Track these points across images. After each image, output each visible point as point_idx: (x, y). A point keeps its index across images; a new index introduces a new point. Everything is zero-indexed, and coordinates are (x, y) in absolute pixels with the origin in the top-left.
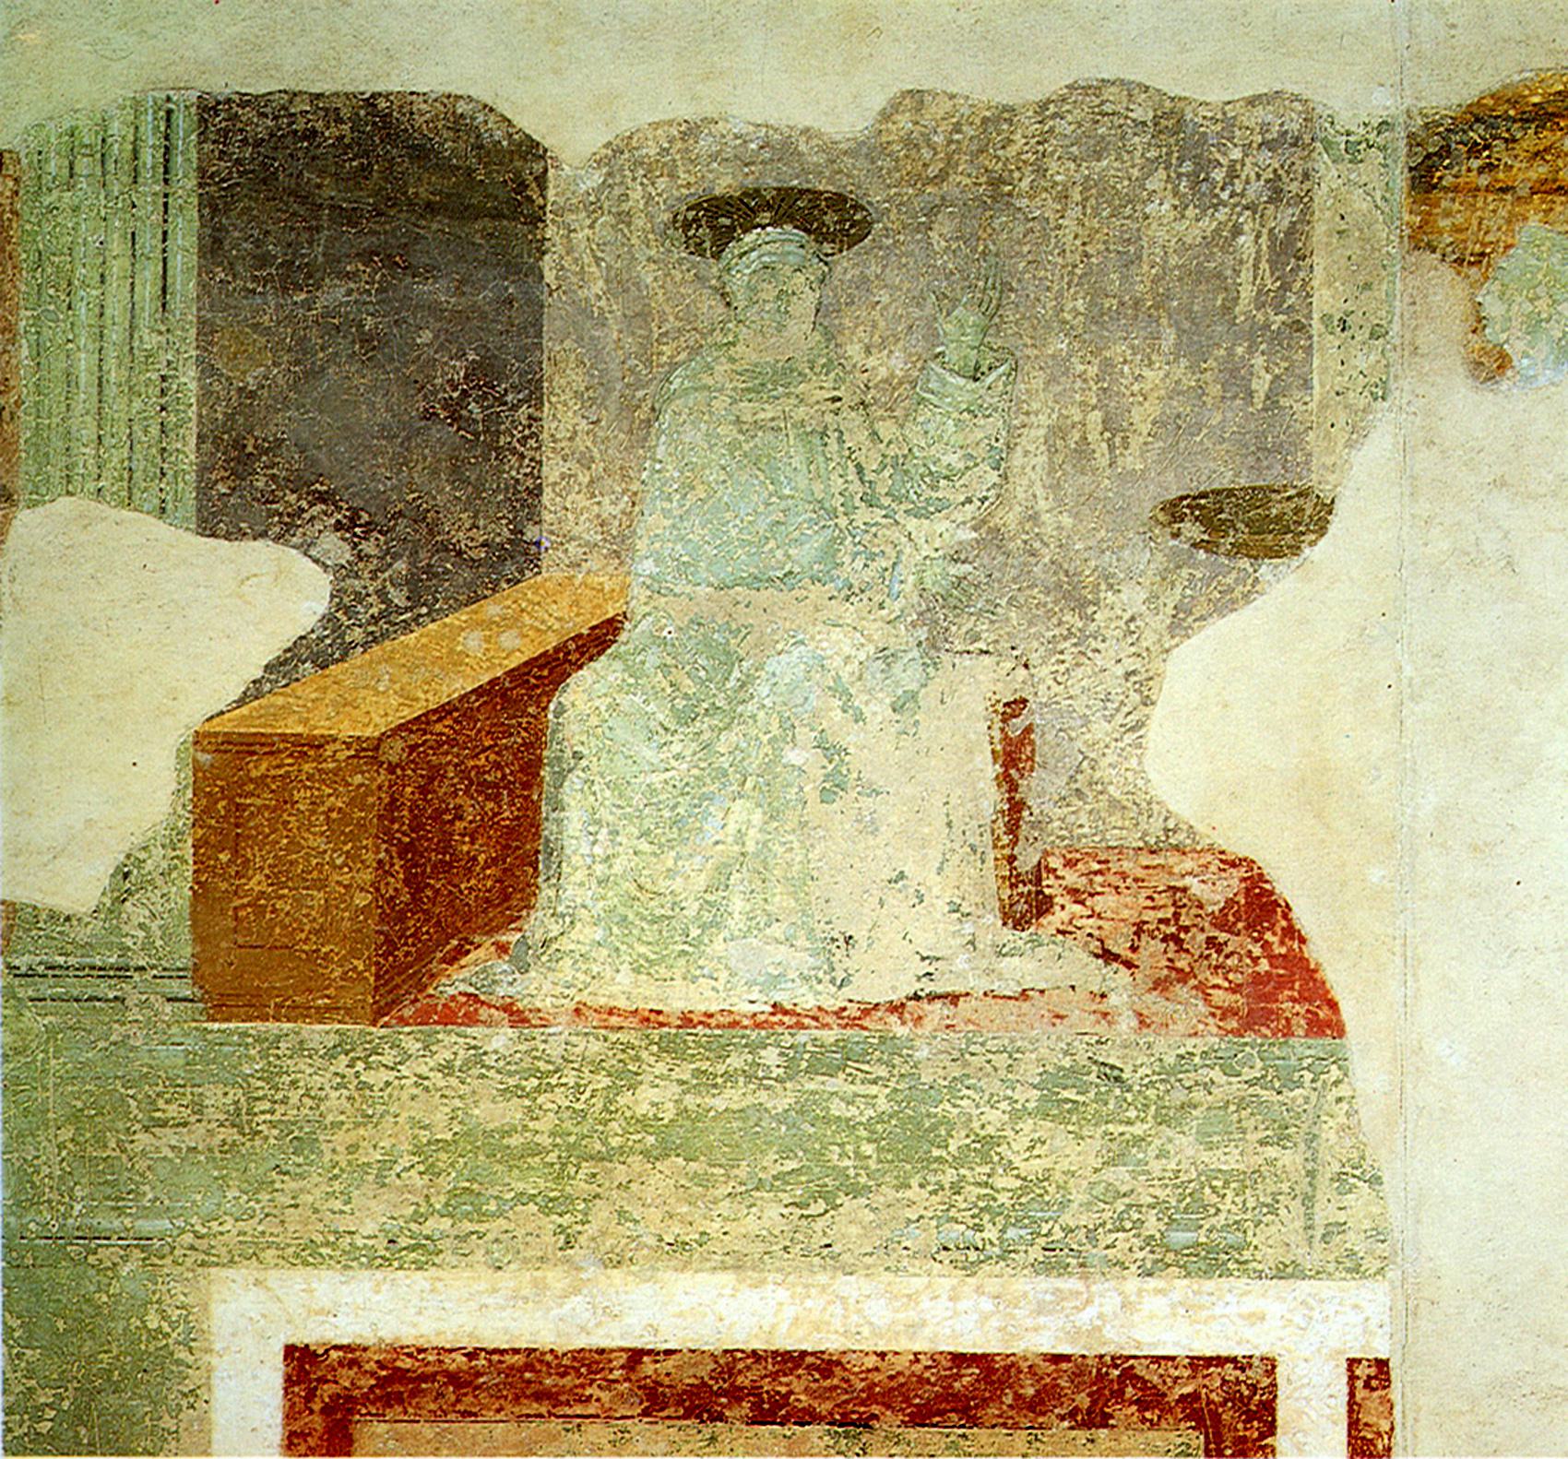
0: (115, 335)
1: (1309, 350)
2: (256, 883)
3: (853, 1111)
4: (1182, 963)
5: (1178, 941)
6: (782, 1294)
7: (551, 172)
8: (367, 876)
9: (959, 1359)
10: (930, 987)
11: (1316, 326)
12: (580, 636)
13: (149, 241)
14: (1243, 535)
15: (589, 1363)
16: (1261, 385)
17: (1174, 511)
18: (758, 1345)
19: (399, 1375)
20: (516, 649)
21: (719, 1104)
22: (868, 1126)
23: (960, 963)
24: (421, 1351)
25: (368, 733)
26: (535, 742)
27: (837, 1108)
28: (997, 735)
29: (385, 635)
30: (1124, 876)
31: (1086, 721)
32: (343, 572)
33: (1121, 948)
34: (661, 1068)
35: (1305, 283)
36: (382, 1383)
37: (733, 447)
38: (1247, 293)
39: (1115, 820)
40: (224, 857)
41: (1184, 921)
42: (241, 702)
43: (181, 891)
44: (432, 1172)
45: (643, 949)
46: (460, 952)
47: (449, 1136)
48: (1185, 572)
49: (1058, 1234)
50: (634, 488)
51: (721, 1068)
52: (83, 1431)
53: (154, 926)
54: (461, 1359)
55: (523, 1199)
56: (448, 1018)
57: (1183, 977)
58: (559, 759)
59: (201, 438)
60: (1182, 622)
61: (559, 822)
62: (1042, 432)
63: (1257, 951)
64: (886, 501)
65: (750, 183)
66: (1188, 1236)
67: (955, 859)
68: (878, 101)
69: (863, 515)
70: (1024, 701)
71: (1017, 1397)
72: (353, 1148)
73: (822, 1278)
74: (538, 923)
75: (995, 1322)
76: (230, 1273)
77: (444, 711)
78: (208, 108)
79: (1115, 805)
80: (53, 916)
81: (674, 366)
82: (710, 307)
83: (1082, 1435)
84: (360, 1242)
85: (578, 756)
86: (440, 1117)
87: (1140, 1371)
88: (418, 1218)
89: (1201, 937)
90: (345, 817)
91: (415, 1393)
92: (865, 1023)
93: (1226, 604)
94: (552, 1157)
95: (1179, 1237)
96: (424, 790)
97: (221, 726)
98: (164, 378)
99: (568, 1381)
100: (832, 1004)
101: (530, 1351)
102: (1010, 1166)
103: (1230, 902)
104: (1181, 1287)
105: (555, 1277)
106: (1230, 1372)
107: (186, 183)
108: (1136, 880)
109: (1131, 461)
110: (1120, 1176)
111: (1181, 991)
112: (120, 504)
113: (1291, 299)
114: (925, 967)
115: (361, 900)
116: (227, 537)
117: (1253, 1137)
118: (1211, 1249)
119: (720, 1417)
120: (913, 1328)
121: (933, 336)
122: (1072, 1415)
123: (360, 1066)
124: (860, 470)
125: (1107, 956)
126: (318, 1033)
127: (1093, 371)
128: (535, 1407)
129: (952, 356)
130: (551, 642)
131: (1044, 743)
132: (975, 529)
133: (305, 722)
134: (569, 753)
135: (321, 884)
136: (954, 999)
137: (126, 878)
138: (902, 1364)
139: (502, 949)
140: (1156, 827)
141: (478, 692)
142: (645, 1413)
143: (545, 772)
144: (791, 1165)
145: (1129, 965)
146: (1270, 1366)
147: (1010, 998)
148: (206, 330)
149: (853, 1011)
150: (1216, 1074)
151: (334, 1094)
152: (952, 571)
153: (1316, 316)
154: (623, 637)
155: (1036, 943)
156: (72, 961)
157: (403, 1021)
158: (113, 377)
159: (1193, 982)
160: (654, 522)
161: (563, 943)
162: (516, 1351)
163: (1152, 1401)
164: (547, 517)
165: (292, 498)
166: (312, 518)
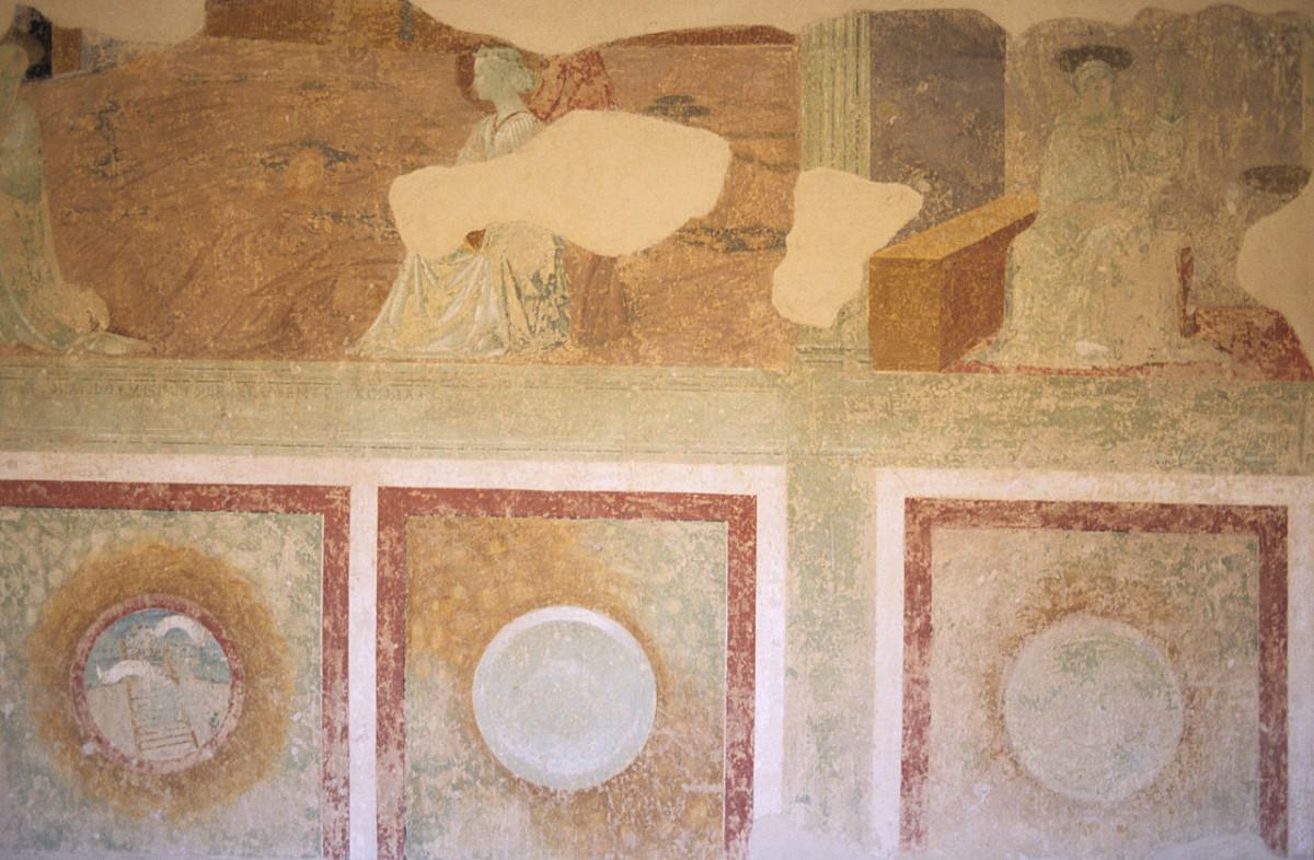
0: (838, 105)
1: (1301, 113)
2: (893, 317)
3: (1122, 409)
4: (1251, 351)
5: (1249, 343)
6: (1095, 481)
7: (1007, 40)
8: (937, 314)
9: (1163, 506)
10: (1152, 360)
11: (1304, 103)
12: (1019, 221)
13: (851, 69)
14: (1275, 184)
15: (1021, 506)
16: (1282, 125)
17: (1247, 175)
18: (1086, 499)
19: (949, 510)
20: (996, 225)
21: (1072, 405)
22: (1129, 414)
23: (1165, 351)
24: (957, 500)
25: (937, 258)
26: (1002, 262)
27: (1116, 407)
28: (1179, 263)
29: (944, 219)
30: (1228, 317)
31: (1213, 256)
32: (928, 195)
33: (1228, 346)
34: (1050, 390)
35: (1300, 85)
36: (943, 513)
37: (1079, 147)
38: (1277, 89)
39: (1225, 295)
40: (881, 306)
41: (1252, 335)
42: (888, 246)
43: (865, 319)
44: (962, 430)
45: (1043, 344)
46: (973, 344)
47: (967, 416)
48: (1253, 198)
49: (1201, 457)
50: (1041, 162)
51: (1073, 391)
52: (826, 531)
53: (854, 333)
54: (973, 505)
55: (996, 441)
56: (969, 370)
57: (1251, 357)
58: (1011, 269)
59: (872, 144)
60: (1250, 219)
61: (1011, 293)
62: (1196, 143)
63: (1280, 347)
64: (1138, 169)
65: (1085, 44)
66: (1253, 459)
67: (1162, 310)
68: (1134, 13)
69: (1129, 175)
70: (1189, 249)
71: (1186, 521)
72: (932, 421)
73: (1110, 474)
74: (1003, 333)
75: (1176, 492)
76: (884, 469)
77: (966, 249)
78: (873, 17)
79: (1224, 290)
80: (814, 329)
81: (1055, 115)
82: (1069, 92)
83: (1210, 536)
84: (934, 457)
85: (1019, 268)
86: (966, 407)
87: (1233, 511)
88: (956, 448)
89: (1259, 342)
90: (928, 291)
91: (956, 517)
92: (1128, 373)
93: (1268, 212)
94: (1008, 425)
95: (1249, 459)
96: (959, 280)
97: (881, 255)
98: (857, 121)
99: (1014, 513)
100: (1115, 366)
101: (999, 502)
102: (1183, 431)
103: (1270, 328)
104: (1250, 479)
105: (1009, 472)
106: (1270, 512)
107: (865, 46)
108: (1233, 319)
109: (1232, 154)
110: (1226, 435)
111: (1251, 363)
112: (841, 169)
113: (1294, 91)
114: (1150, 353)
115: (935, 323)
116: (883, 181)
117: (1279, 420)
118: (1263, 464)
119: (1070, 528)
120: (1146, 493)
121: (1156, 105)
122: (1207, 528)
123: (934, 389)
124: (1128, 156)
125: (1221, 349)
126: (918, 375)
127: (1217, 119)
128: (999, 523)
129: (1164, 112)
130: (1008, 222)
131: (1198, 263)
132: (1172, 180)
133: (913, 253)
134: (1015, 267)
135: (919, 317)
136: (1162, 365)
137: (843, 315)
138: (1141, 507)
139: (989, 343)
140: (1240, 299)
141: (980, 242)
142: (1043, 526)
143: (1007, 274)
144: (1099, 429)
145: (1230, 352)
146: (1285, 510)
147: (1182, 365)
148: (874, 103)
149: (1123, 369)
150: (1265, 395)
151: (924, 399)
152: (1163, 197)
153: (1304, 98)
154: (1036, 221)
155: (1193, 343)
156: (823, 347)
157: (951, 371)
158: (838, 120)
159: (1255, 359)
160: (1048, 176)
161: (1013, 342)
162: (993, 501)
163: (1237, 522)
164: (1007, 174)
165: (907, 166)
166: (915, 175)
